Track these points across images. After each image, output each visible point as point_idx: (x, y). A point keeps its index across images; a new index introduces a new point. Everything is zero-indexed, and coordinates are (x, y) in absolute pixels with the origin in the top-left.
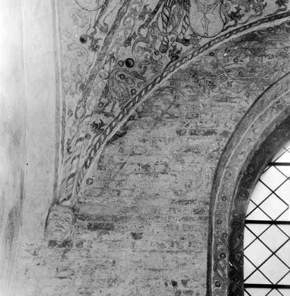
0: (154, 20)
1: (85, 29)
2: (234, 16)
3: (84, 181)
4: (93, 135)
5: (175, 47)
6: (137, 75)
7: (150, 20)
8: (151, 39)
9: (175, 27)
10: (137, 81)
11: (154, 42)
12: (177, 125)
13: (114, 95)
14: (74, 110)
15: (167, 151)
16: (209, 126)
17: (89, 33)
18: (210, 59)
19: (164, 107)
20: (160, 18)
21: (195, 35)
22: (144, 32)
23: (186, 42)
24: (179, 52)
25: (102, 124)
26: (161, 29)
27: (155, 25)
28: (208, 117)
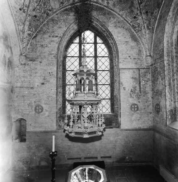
0: (40, 3)
1: (20, 6)
2: (62, 3)
3: (27, 49)
4: (28, 37)
5: (47, 12)
6: (38, 20)
7: (39, 3)
8: (41, 9)
9: (47, 6)
10: (38, 22)
11: (41, 10)
12: (49, 35)
13: (33, 26)
14: (22, 30)
15: (47, 41)
16: (57, 35)
17: (22, 8)
18: (56, 16)
19: (45, 29)
20: (42, 3)
21: (52, 8)
22: (38, 7)
23: (50, 10)
24: (48, 13)
25: (30, 34)
26: (43, 6)
27: (41, 5)
28: (56, 32)
